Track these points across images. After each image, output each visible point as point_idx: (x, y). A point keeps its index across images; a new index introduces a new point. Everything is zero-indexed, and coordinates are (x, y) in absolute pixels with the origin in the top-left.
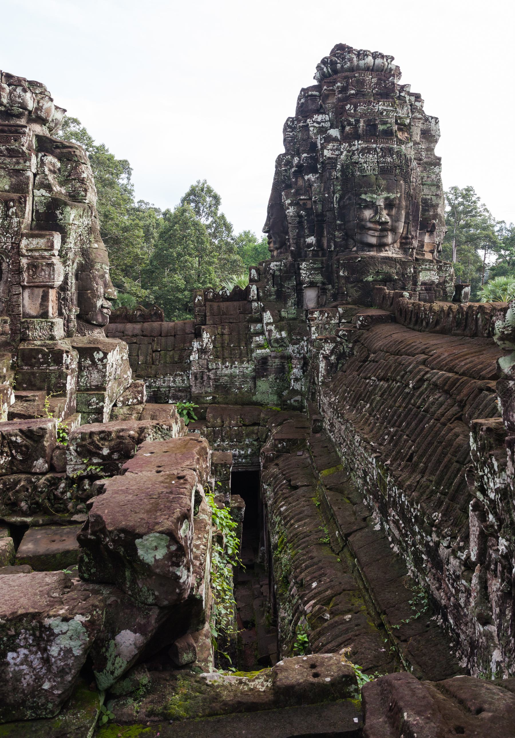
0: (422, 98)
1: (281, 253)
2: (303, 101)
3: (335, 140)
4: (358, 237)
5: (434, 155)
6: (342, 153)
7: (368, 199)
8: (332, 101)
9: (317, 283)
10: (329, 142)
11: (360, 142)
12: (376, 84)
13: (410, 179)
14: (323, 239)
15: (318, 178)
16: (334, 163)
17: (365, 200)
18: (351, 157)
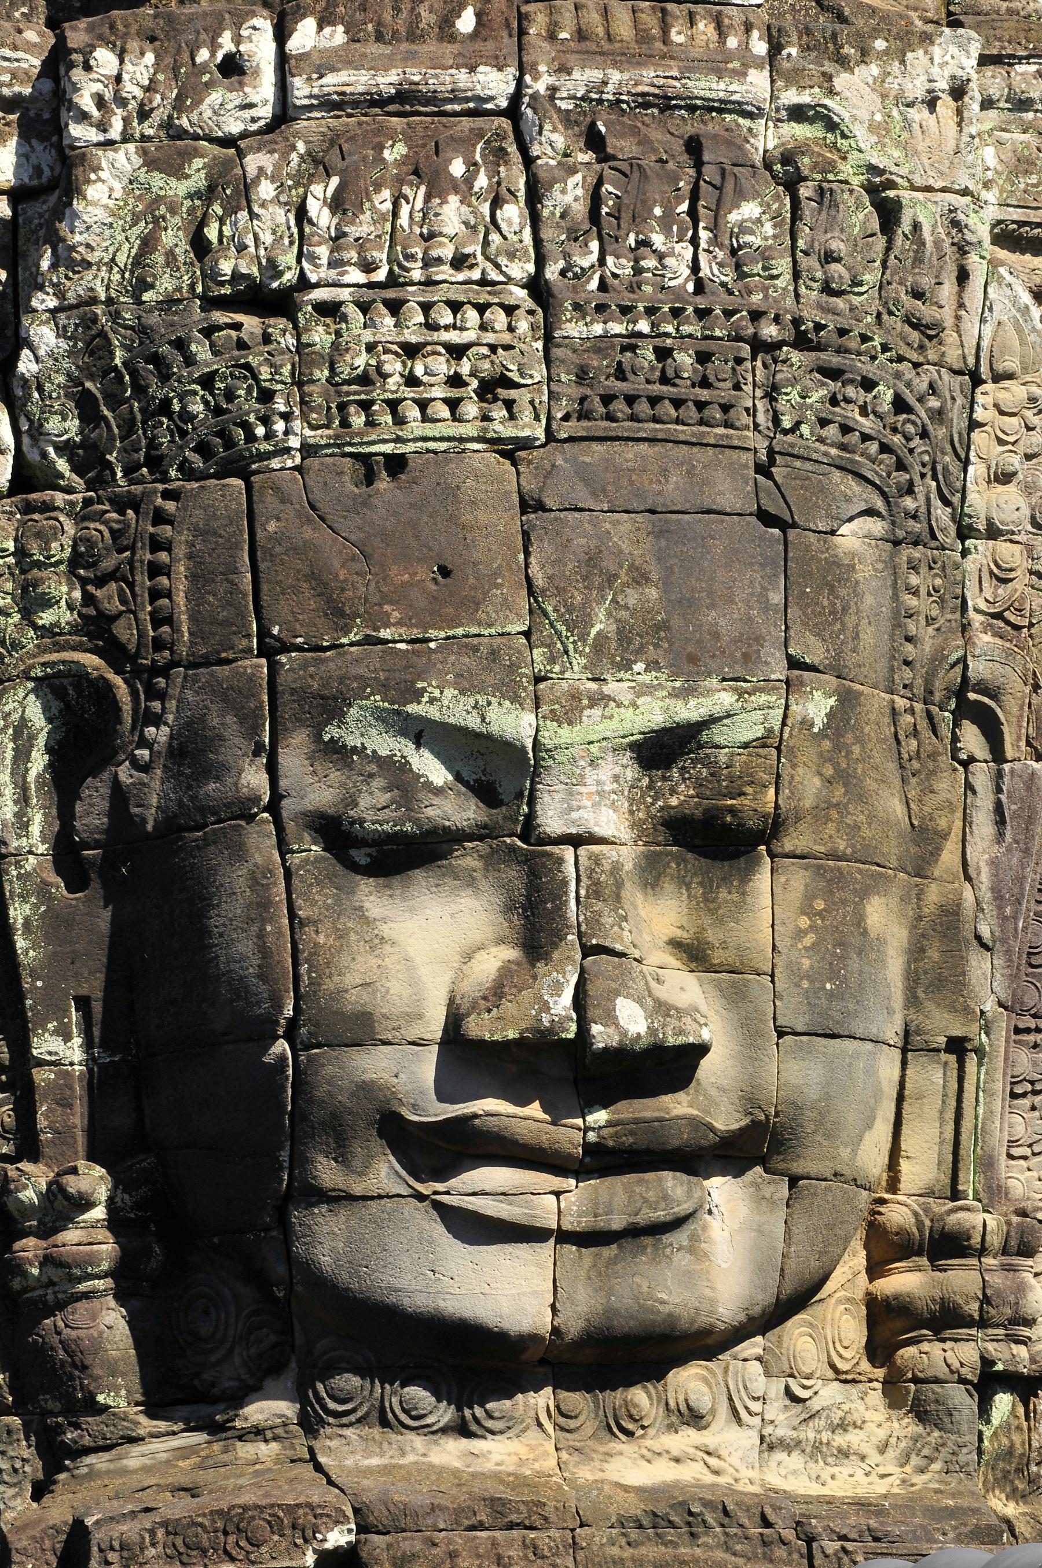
11: (305, 36)
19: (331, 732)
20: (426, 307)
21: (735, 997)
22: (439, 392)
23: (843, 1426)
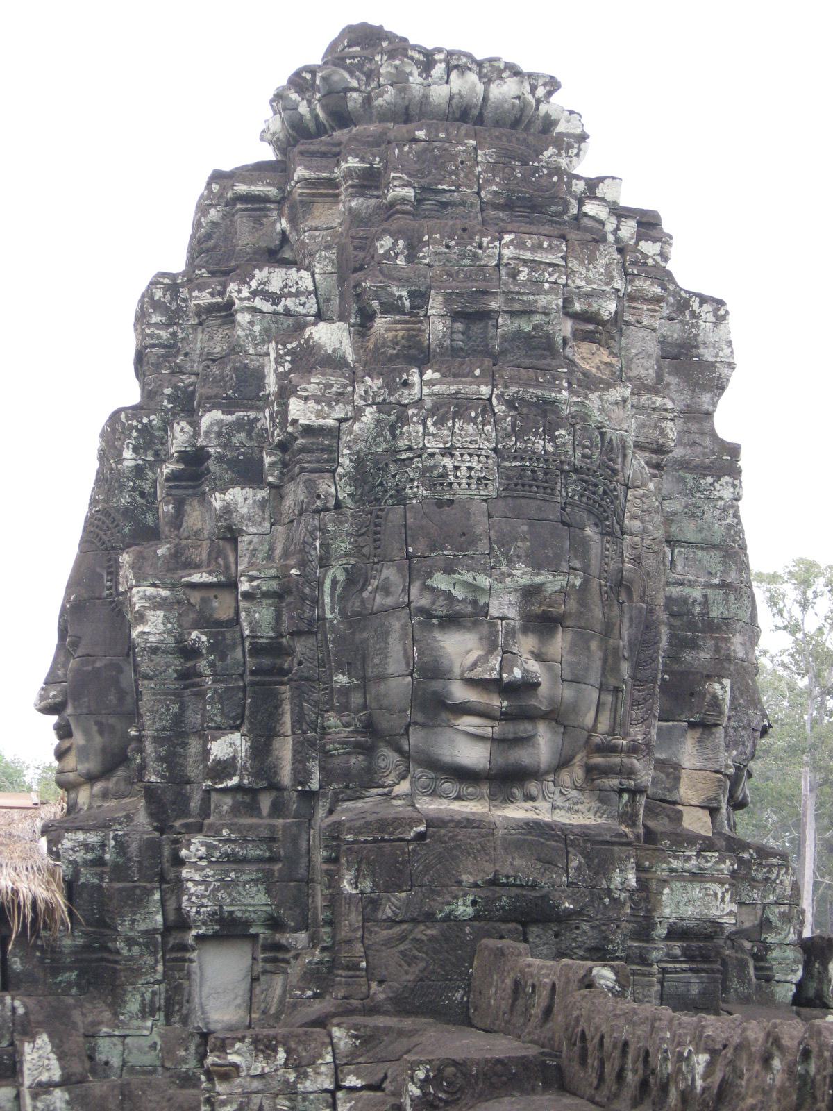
0: (666, 226)
1: (105, 795)
2: (214, 214)
3: (333, 362)
4: (416, 738)
5: (713, 434)
6: (359, 411)
7: (458, 593)
8: (329, 218)
9: (247, 924)
10: (309, 371)
11: (429, 375)
12: (493, 168)
13: (620, 522)
14: (277, 743)
15: (263, 504)
16: (329, 450)
17: (448, 596)
18: (393, 427)
19: (429, 582)
20: (462, 455)
21: (550, 670)
22: (464, 481)
23: (577, 803)
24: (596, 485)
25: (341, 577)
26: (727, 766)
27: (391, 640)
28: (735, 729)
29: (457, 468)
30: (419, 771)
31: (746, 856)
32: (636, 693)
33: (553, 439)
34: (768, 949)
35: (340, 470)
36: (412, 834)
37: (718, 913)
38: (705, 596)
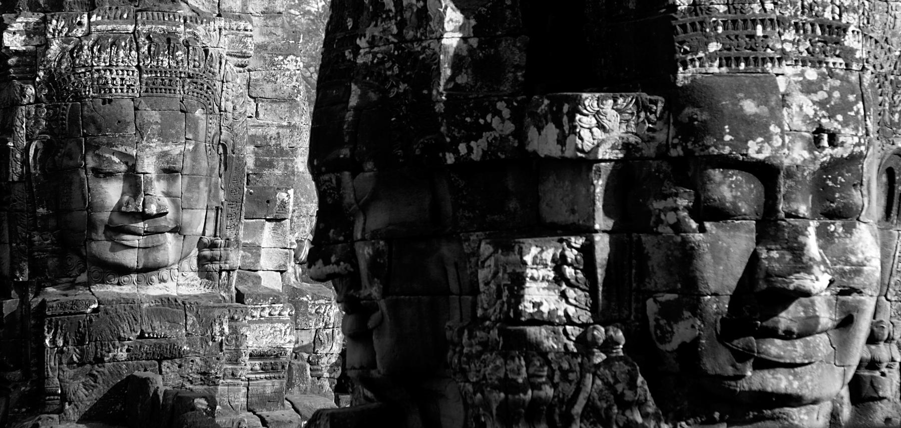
19: (97, 152)
24: (202, 84)
25: (40, 147)
26: (291, 244)
27: (73, 188)
28: (298, 217)
29: (114, 79)
30: (93, 268)
31: (305, 299)
32: (230, 209)
33: (174, 57)
34: (320, 358)
35: (38, 79)
36: (89, 310)
37: (282, 342)
38: (278, 133)
